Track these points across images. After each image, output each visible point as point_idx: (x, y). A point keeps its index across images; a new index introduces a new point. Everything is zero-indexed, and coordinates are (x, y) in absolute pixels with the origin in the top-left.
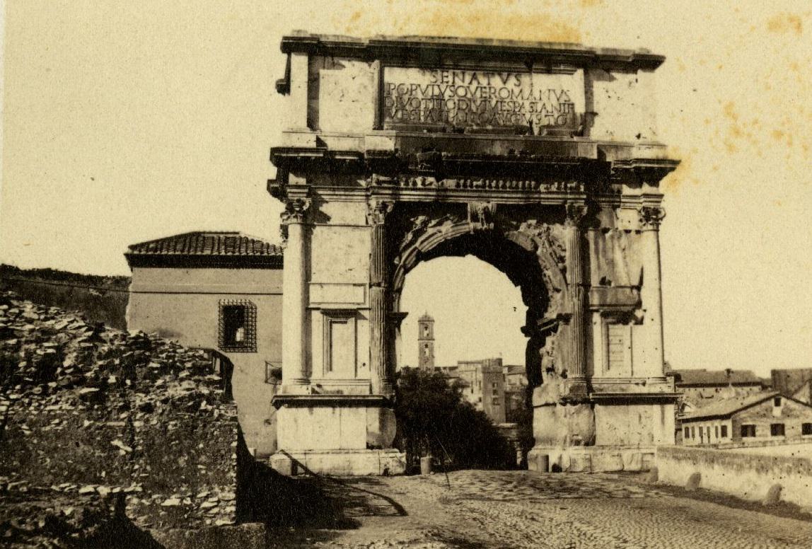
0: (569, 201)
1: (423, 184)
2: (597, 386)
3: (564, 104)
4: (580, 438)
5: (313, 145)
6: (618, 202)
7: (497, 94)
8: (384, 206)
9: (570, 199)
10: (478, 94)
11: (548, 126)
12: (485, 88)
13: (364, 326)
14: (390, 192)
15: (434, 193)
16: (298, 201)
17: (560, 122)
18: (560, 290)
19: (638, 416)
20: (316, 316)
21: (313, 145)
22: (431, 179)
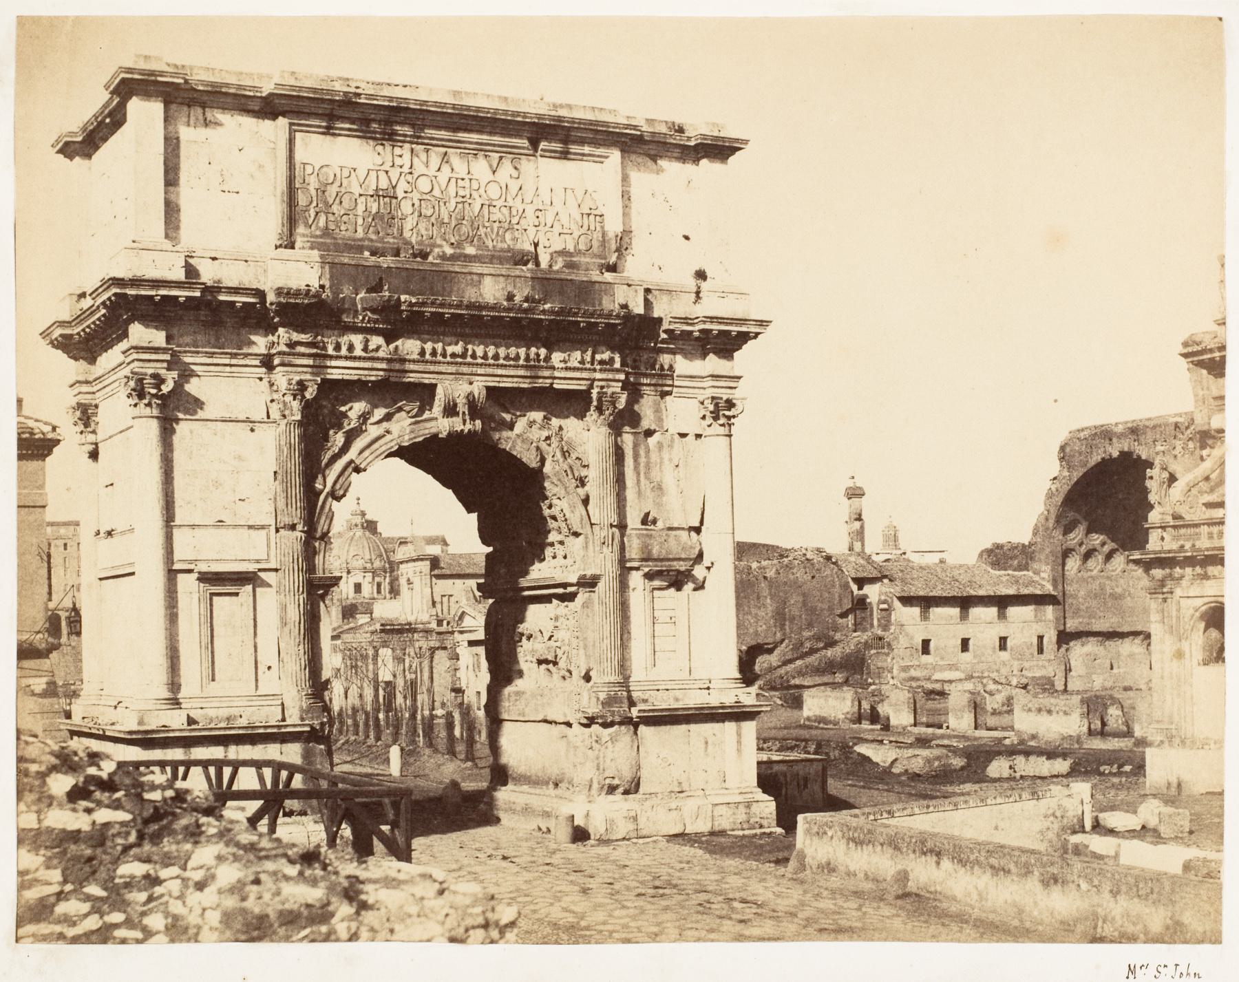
0: (596, 383)
1: (365, 349)
2: (639, 694)
3: (589, 215)
4: (616, 782)
5: (180, 275)
6: (669, 386)
7: (482, 191)
8: (302, 386)
9: (599, 380)
10: (452, 190)
11: (563, 253)
12: (463, 179)
13: (268, 599)
14: (311, 362)
15: (384, 366)
16: (154, 376)
17: (582, 247)
18: (580, 534)
19: (703, 741)
20: (188, 585)
21: (180, 275)
22: (376, 341)
